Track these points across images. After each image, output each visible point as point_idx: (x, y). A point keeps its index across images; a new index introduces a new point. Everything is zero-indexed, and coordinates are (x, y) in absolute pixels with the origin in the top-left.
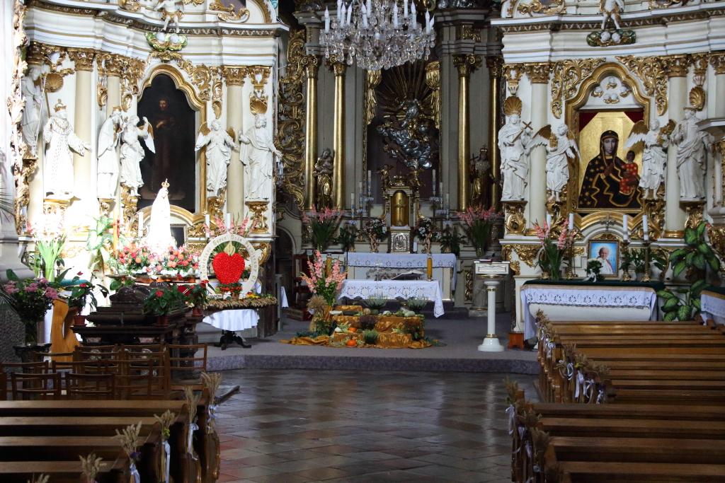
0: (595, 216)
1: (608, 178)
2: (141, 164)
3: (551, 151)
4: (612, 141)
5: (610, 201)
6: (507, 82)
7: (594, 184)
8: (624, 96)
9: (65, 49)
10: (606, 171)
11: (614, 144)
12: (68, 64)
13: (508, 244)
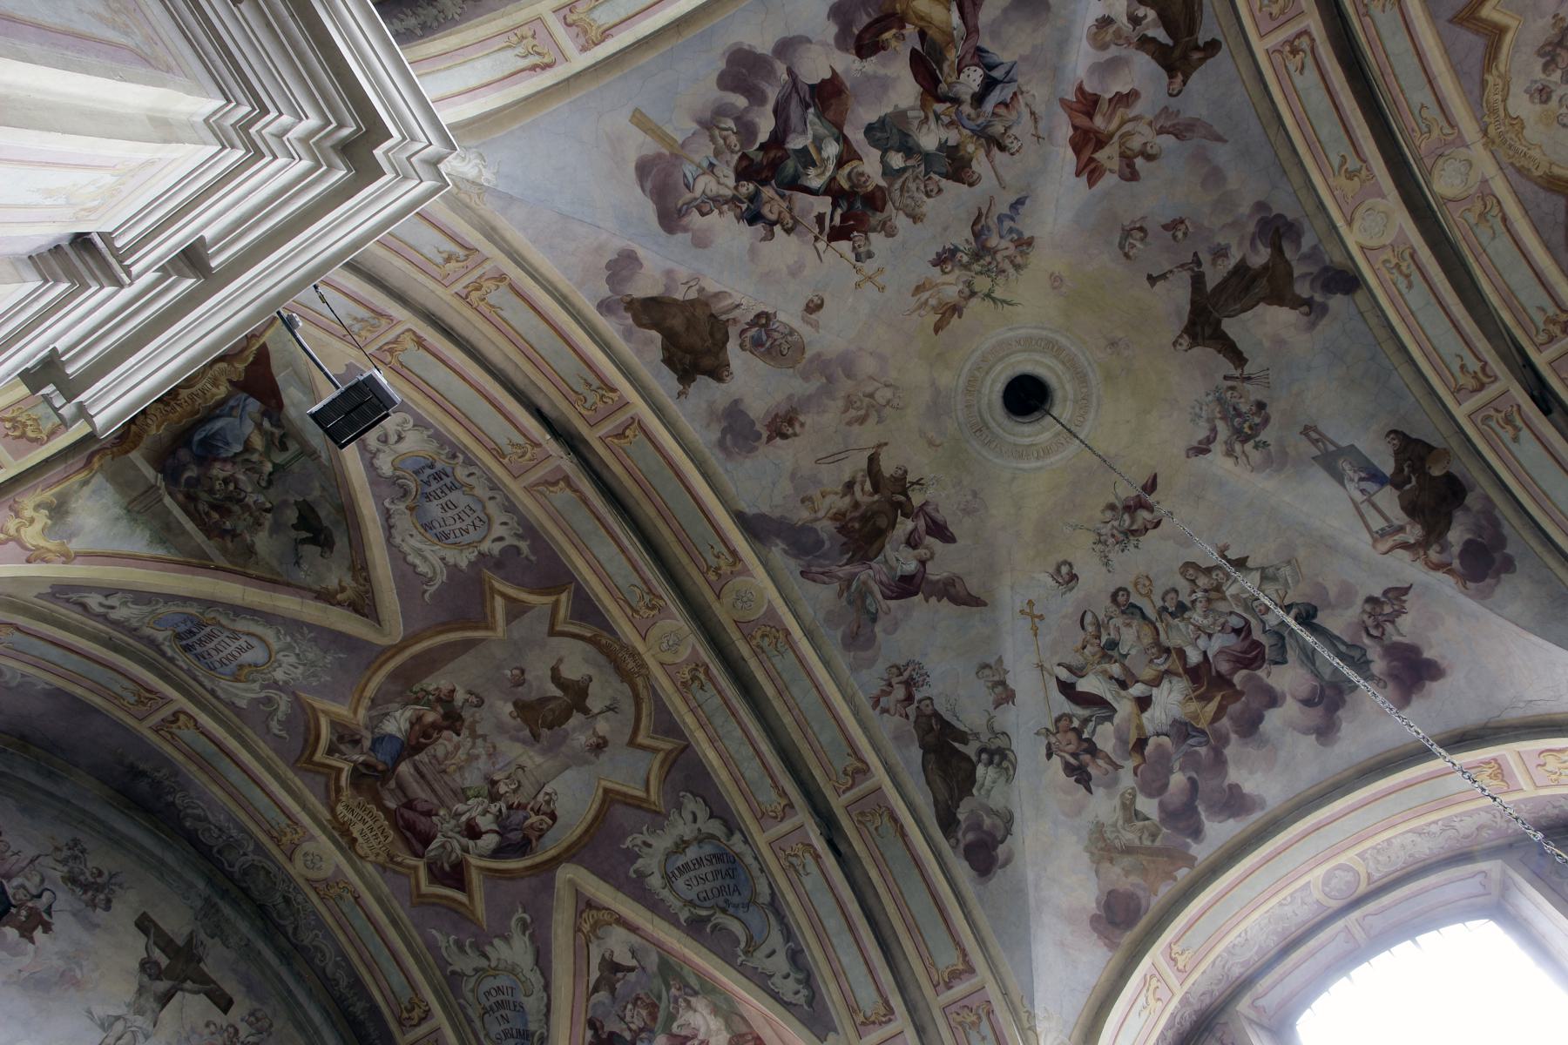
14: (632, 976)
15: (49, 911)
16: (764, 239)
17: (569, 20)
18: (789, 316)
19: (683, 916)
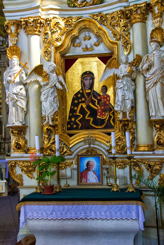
0: (80, 136)
1: (89, 107)
3: (44, 85)
4: (90, 79)
5: (91, 124)
6: (9, 37)
7: (78, 111)
8: (96, 45)
10: (86, 101)
11: (91, 81)
13: (13, 161)
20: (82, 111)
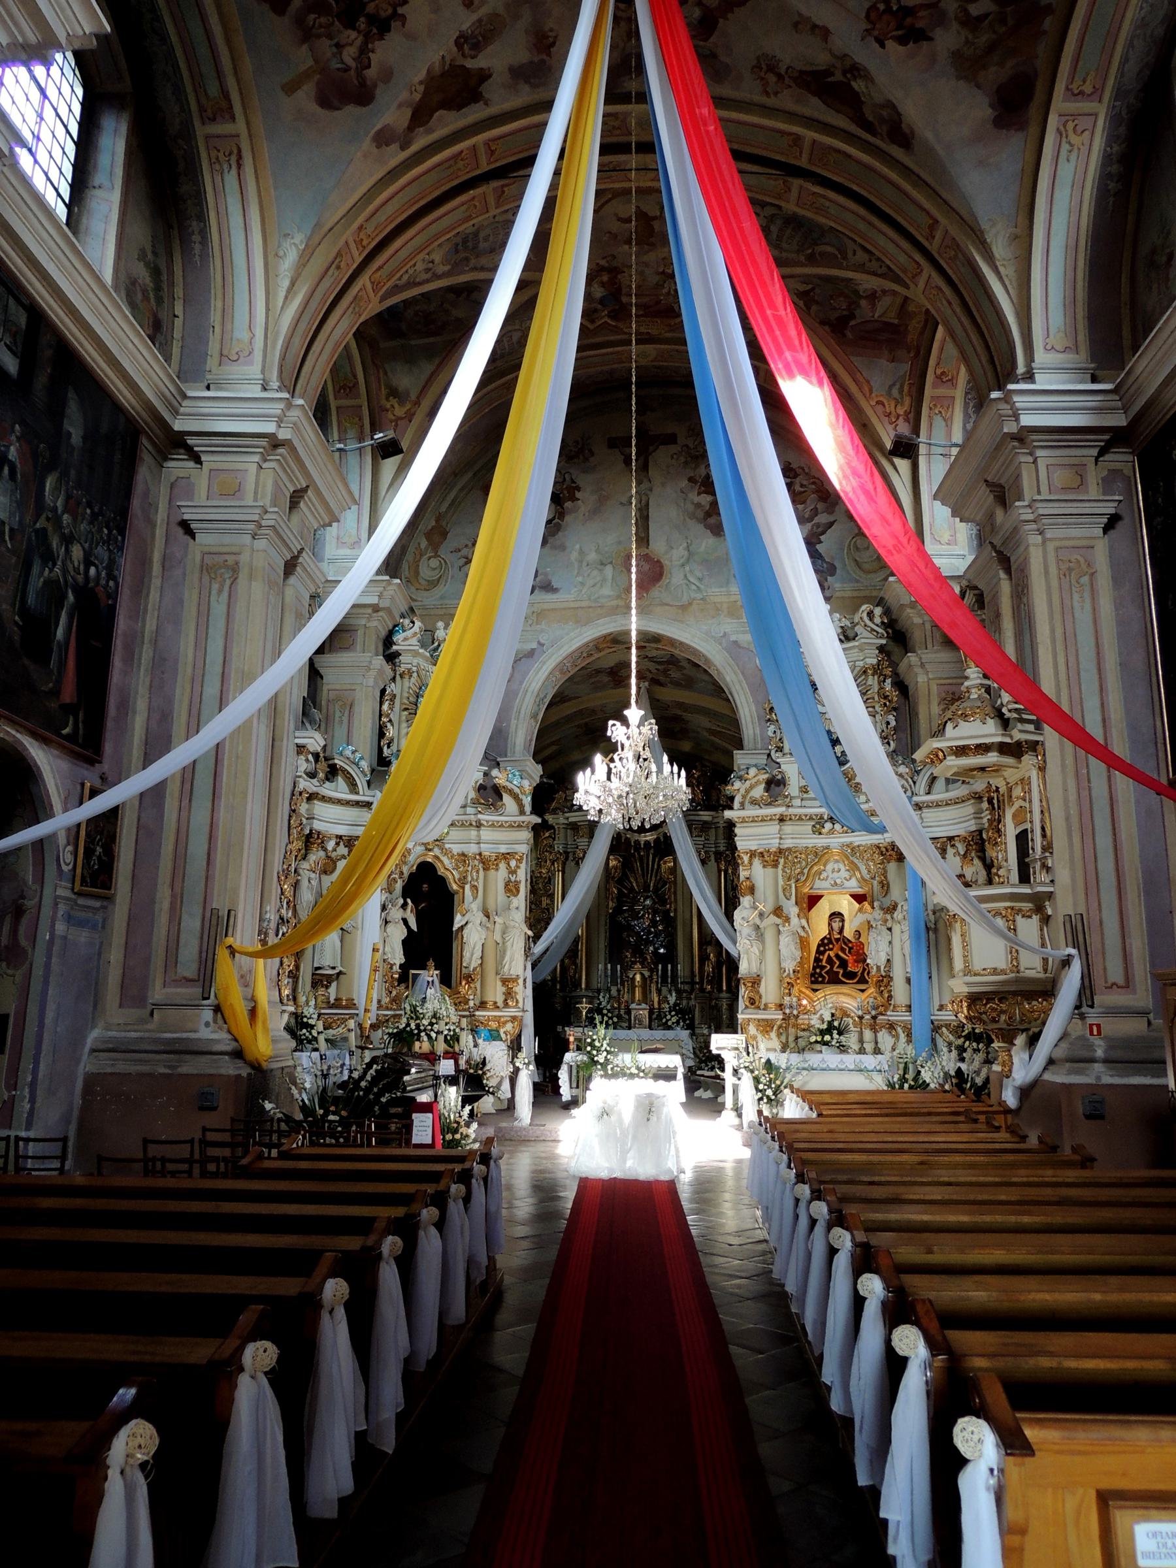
2: (404, 942)
9: (340, 837)
12: (342, 850)
14: (817, 291)
15: (573, 482)
16: (403, 25)
17: (211, 116)
18: (467, 21)
19: (802, 258)
20: (830, 961)
